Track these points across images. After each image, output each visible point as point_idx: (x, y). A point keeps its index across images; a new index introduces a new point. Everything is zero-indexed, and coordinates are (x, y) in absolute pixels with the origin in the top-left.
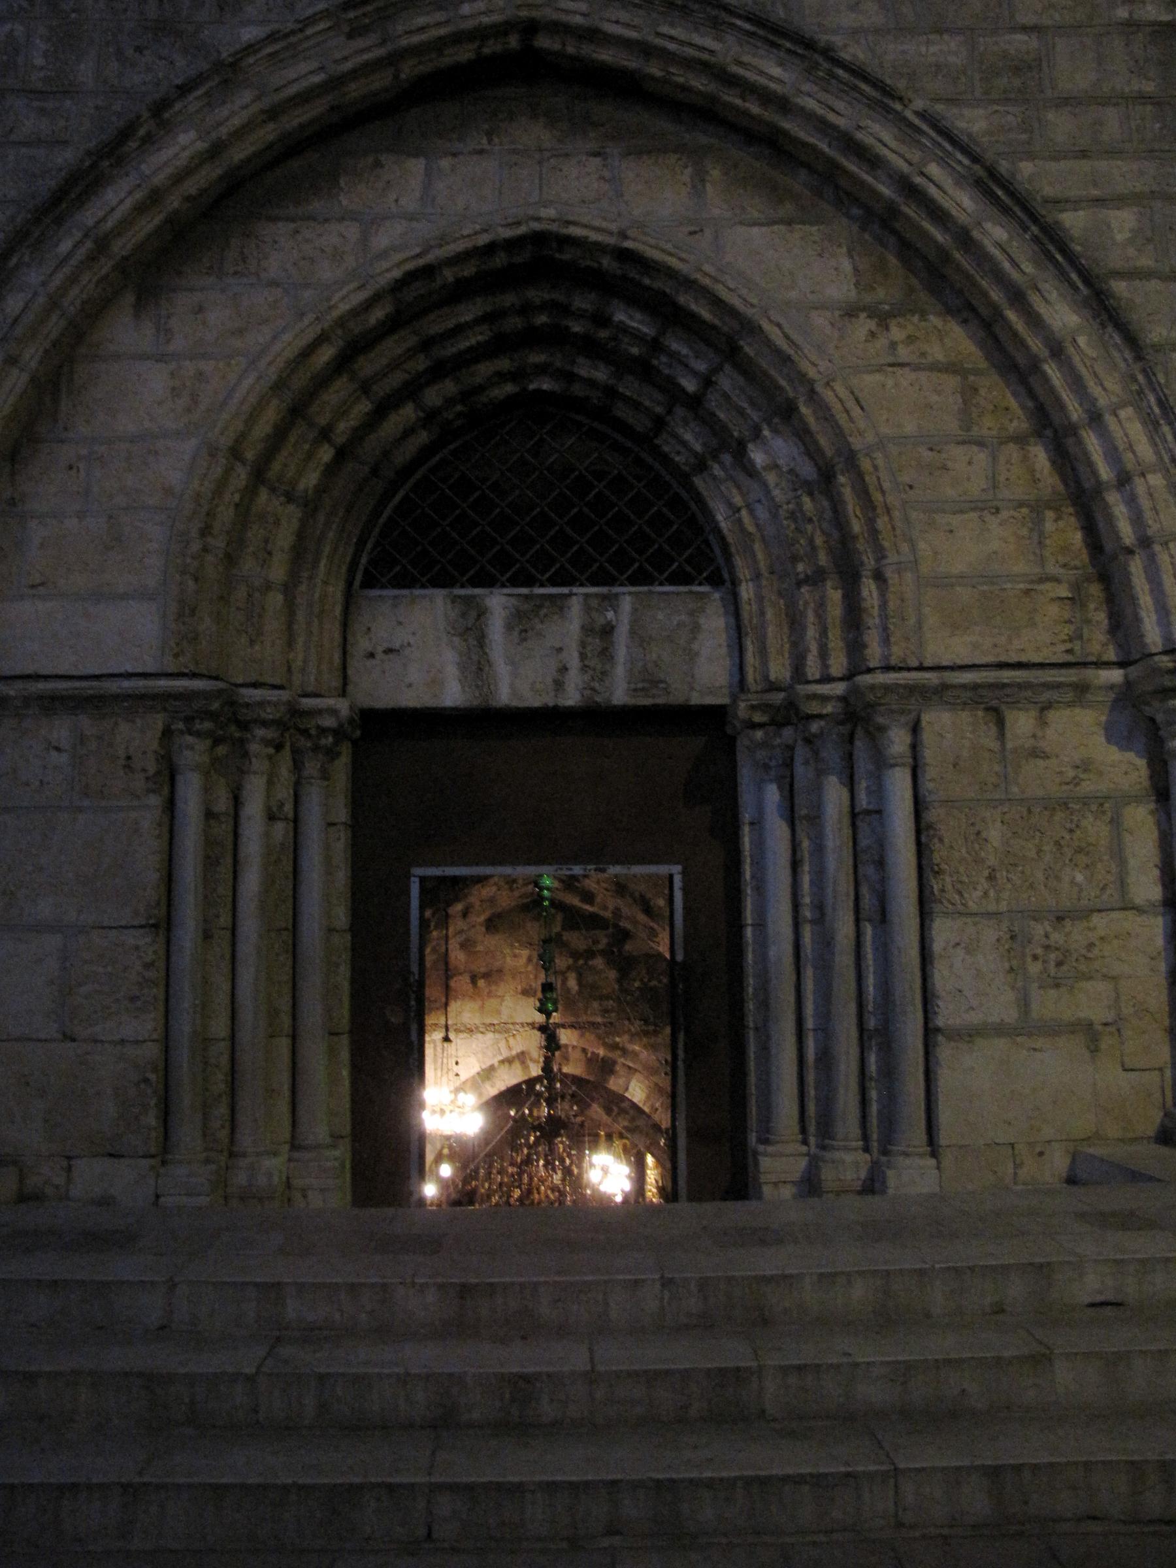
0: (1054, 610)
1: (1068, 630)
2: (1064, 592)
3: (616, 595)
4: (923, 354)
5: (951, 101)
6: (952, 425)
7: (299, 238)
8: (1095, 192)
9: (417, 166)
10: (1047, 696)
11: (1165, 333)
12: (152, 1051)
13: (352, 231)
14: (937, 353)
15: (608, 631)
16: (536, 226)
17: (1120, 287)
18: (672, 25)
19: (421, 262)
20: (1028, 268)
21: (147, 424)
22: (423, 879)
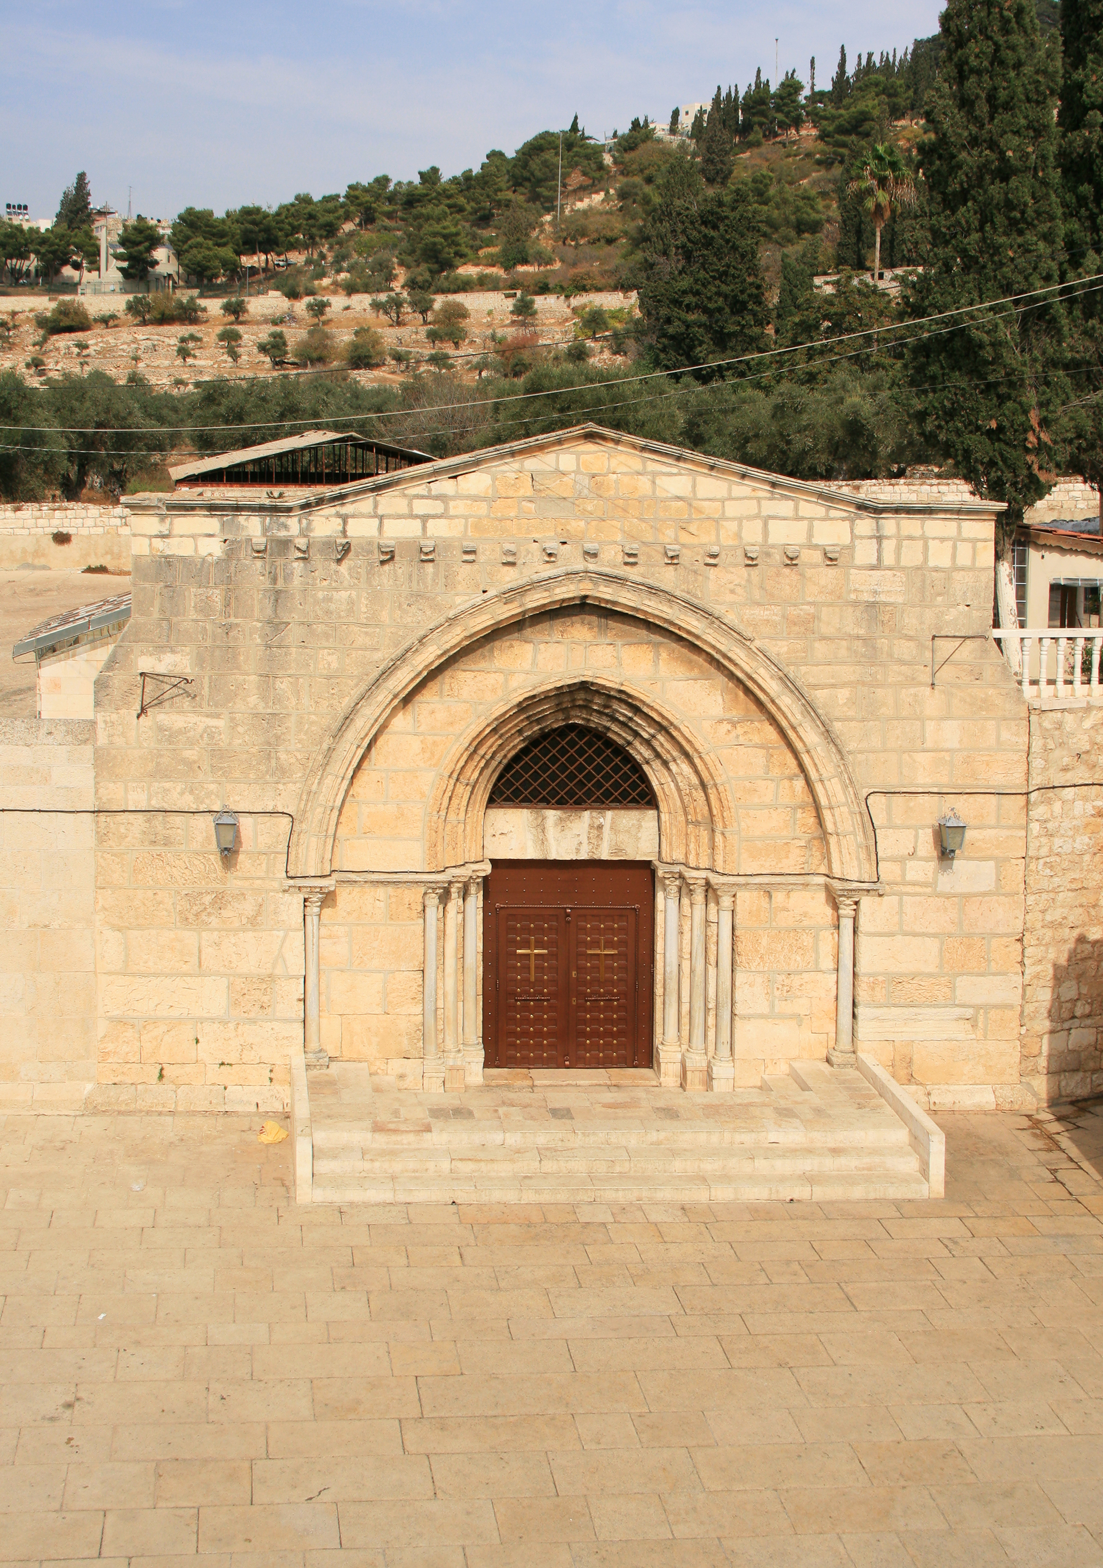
17: (837, 726)
20: (799, 717)
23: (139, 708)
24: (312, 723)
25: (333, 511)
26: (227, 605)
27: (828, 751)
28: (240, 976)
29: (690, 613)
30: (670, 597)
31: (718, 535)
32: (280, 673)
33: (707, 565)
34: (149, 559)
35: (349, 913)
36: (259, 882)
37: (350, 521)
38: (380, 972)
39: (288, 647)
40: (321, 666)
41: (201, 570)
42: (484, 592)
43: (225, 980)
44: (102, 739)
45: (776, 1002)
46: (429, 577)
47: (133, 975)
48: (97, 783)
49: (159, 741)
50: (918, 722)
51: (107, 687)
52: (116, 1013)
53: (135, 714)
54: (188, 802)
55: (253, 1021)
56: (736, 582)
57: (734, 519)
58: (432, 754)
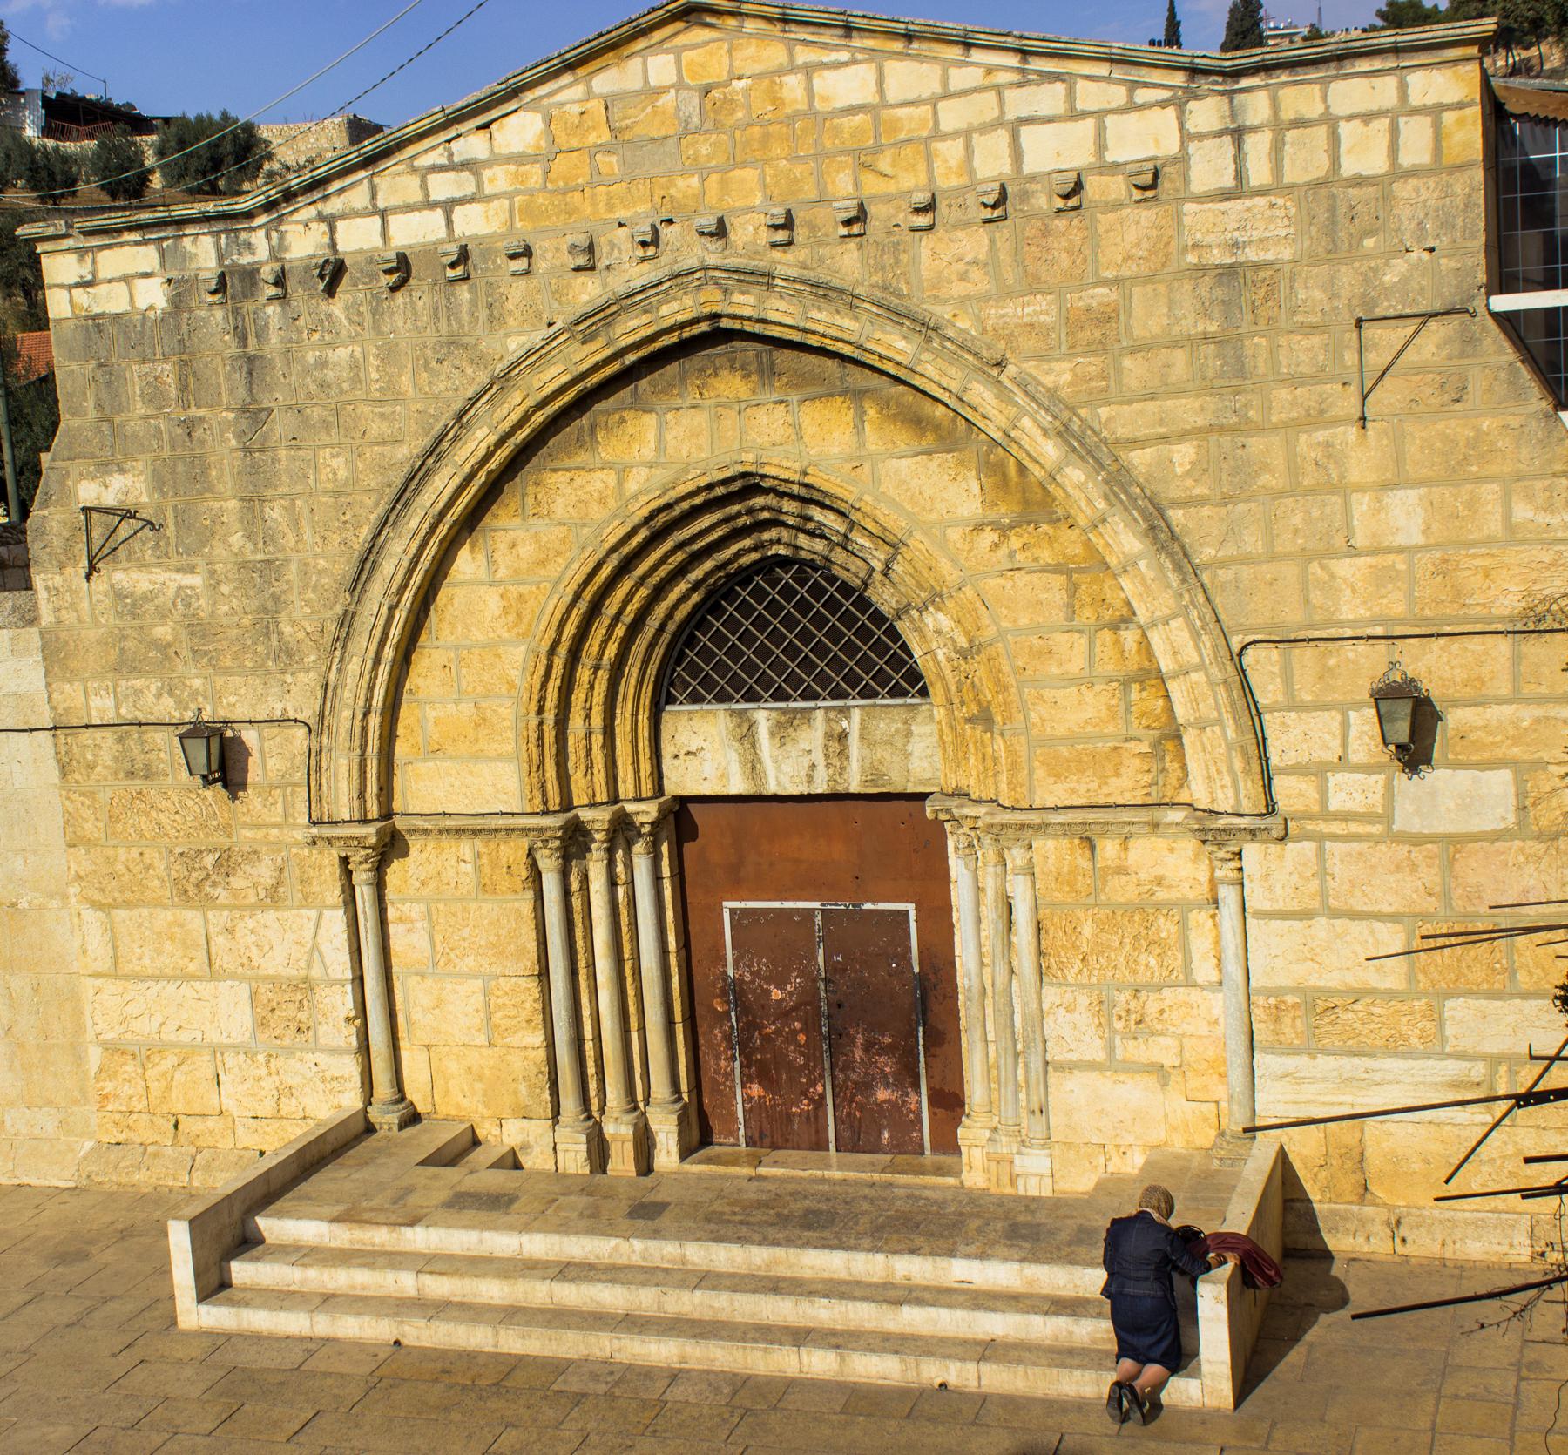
0: (1137, 762)
1: (1147, 778)
2: (1145, 748)
3: (849, 708)
4: (1036, 559)
5: (1040, 358)
6: (1058, 616)
7: (575, 484)
8: (1163, 430)
9: (650, 420)
10: (1126, 830)
11: (1213, 552)
12: (541, 1055)
13: (611, 478)
14: (1046, 556)
15: (843, 736)
16: (742, 469)
17: (1176, 515)
18: (819, 309)
19: (661, 502)
21: (491, 635)
22: (733, 911)
23: (86, 563)
24: (320, 572)
25: (312, 211)
26: (184, 388)
27: (1161, 567)
28: (266, 978)
29: (889, 327)
30: (850, 300)
31: (930, 171)
32: (269, 493)
33: (914, 229)
34: (71, 323)
35: (423, 883)
36: (275, 832)
37: (340, 225)
38: (476, 977)
39: (274, 449)
40: (323, 477)
41: (142, 333)
42: (550, 325)
43: (245, 986)
44: (46, 617)
45: (1118, 1041)
46: (465, 309)
47: (126, 977)
48: (48, 685)
49: (119, 615)
50: (1334, 498)
51: (43, 533)
52: (109, 1036)
53: (83, 573)
54: (167, 708)
55: (290, 1052)
56: (969, 258)
57: (954, 135)
58: (519, 615)
